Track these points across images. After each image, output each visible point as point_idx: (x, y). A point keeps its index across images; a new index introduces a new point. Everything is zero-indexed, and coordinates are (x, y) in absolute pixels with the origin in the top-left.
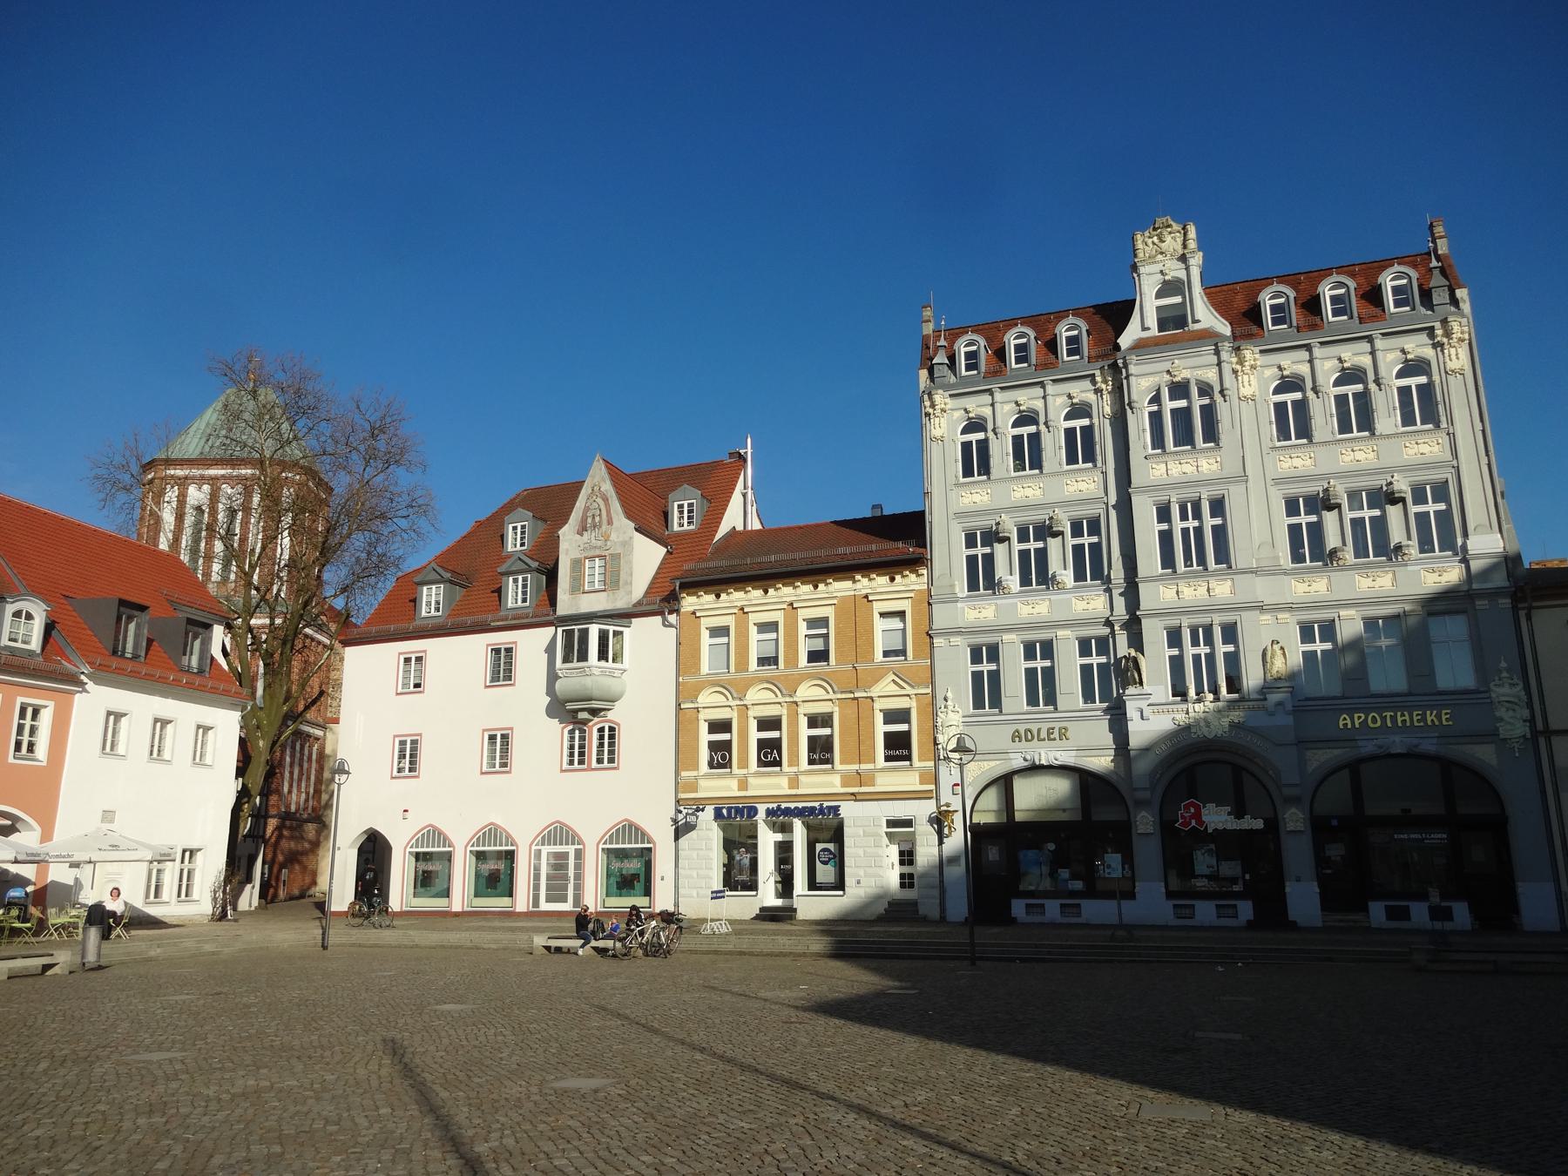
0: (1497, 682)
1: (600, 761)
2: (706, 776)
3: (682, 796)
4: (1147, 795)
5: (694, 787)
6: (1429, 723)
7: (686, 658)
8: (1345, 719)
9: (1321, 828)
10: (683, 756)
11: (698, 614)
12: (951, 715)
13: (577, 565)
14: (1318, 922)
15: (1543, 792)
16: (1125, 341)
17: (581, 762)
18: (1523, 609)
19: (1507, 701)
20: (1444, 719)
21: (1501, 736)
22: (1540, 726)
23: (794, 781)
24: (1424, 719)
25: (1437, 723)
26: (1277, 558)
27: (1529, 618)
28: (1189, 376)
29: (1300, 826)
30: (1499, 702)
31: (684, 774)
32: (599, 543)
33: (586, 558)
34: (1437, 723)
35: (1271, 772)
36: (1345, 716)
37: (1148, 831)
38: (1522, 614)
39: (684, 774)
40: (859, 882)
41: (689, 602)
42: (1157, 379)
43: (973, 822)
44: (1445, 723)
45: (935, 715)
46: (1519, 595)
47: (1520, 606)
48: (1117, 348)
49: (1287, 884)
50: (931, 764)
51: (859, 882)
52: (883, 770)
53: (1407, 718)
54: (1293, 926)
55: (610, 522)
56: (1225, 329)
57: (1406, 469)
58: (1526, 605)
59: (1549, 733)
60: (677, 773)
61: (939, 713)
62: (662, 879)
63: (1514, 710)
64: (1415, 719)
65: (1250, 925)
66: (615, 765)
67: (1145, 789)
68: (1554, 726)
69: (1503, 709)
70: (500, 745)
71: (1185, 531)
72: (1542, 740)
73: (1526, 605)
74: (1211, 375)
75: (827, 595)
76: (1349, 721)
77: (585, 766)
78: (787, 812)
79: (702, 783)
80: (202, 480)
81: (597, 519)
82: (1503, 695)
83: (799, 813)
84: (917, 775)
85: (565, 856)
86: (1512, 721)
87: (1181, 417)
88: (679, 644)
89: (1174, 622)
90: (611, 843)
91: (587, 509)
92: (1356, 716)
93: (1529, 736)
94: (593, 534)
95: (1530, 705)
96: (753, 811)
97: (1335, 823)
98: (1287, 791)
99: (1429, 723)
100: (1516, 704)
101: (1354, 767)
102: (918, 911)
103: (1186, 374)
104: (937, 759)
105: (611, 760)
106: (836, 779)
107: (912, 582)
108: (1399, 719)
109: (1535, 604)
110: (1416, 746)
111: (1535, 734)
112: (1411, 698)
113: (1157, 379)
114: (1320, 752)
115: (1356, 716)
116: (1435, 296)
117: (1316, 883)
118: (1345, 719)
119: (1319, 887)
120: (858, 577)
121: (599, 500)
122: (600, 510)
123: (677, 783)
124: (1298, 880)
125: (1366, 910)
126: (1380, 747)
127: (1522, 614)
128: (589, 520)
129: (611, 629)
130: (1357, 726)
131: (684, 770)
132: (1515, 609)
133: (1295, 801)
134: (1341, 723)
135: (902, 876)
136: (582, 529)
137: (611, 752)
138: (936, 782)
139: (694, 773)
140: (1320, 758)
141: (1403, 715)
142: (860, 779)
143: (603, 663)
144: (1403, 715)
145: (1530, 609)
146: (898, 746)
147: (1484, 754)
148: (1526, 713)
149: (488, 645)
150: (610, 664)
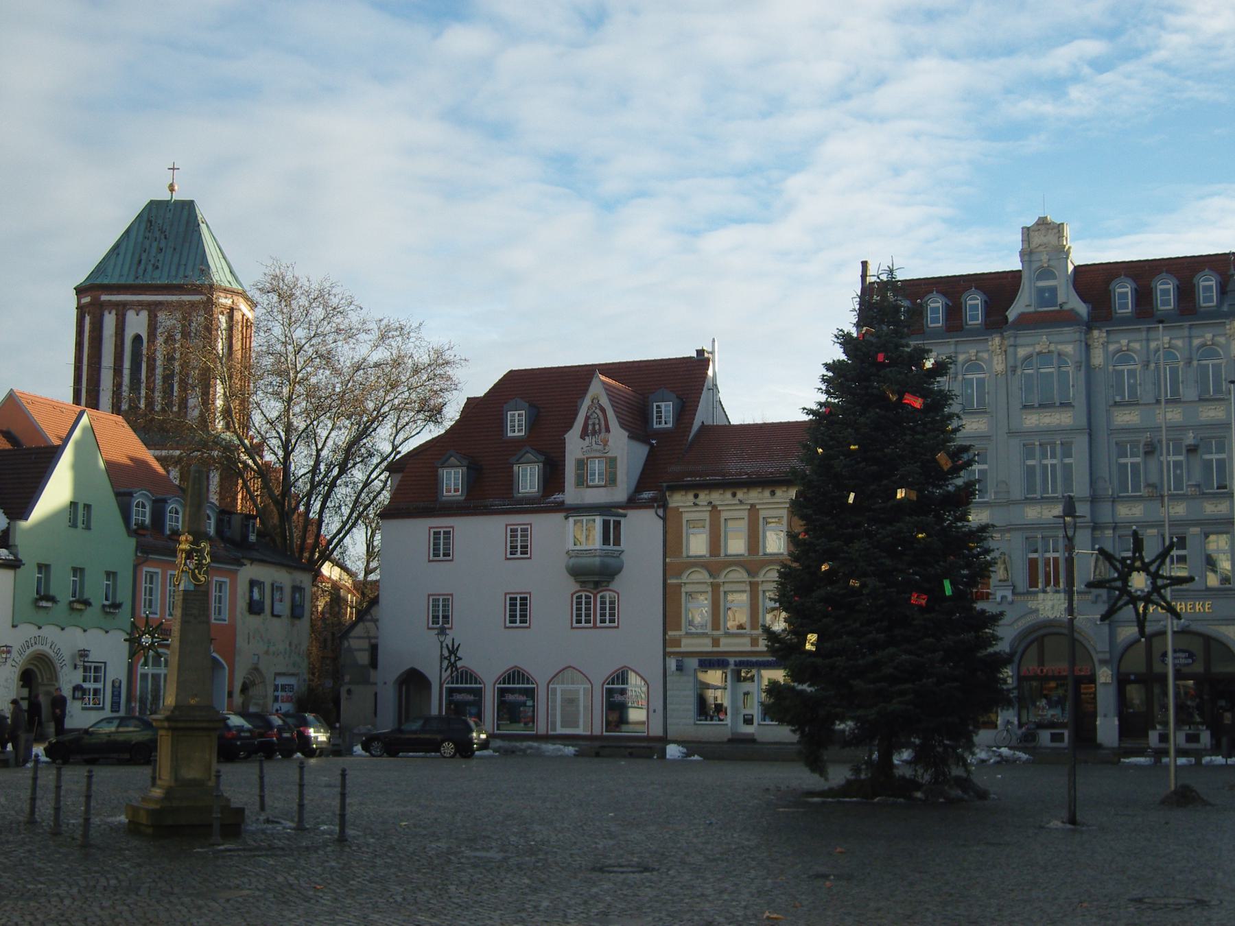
1: (603, 621)
3: (668, 650)
5: (677, 642)
6: (1197, 610)
7: (672, 543)
9: (1122, 682)
13: (581, 464)
16: (1012, 314)
17: (588, 621)
24: (1194, 607)
25: (1202, 610)
29: (1109, 680)
32: (599, 447)
33: (587, 459)
34: (1202, 610)
39: (670, 633)
44: (1207, 610)
53: (1183, 606)
54: (1100, 746)
55: (608, 430)
56: (1082, 309)
62: (654, 711)
64: (1189, 607)
70: (518, 609)
74: (1069, 349)
77: (591, 625)
79: (684, 641)
80: (140, 305)
81: (597, 427)
89: (1029, 534)
91: (587, 418)
94: (594, 440)
97: (1132, 677)
99: (1197, 610)
103: (1052, 347)
105: (612, 621)
110: (1188, 626)
114: (1127, 629)
121: (598, 411)
122: (599, 420)
123: (665, 640)
125: (1147, 736)
129: (612, 519)
136: (584, 434)
137: (612, 615)
143: (606, 547)
149: (507, 526)
150: (611, 547)
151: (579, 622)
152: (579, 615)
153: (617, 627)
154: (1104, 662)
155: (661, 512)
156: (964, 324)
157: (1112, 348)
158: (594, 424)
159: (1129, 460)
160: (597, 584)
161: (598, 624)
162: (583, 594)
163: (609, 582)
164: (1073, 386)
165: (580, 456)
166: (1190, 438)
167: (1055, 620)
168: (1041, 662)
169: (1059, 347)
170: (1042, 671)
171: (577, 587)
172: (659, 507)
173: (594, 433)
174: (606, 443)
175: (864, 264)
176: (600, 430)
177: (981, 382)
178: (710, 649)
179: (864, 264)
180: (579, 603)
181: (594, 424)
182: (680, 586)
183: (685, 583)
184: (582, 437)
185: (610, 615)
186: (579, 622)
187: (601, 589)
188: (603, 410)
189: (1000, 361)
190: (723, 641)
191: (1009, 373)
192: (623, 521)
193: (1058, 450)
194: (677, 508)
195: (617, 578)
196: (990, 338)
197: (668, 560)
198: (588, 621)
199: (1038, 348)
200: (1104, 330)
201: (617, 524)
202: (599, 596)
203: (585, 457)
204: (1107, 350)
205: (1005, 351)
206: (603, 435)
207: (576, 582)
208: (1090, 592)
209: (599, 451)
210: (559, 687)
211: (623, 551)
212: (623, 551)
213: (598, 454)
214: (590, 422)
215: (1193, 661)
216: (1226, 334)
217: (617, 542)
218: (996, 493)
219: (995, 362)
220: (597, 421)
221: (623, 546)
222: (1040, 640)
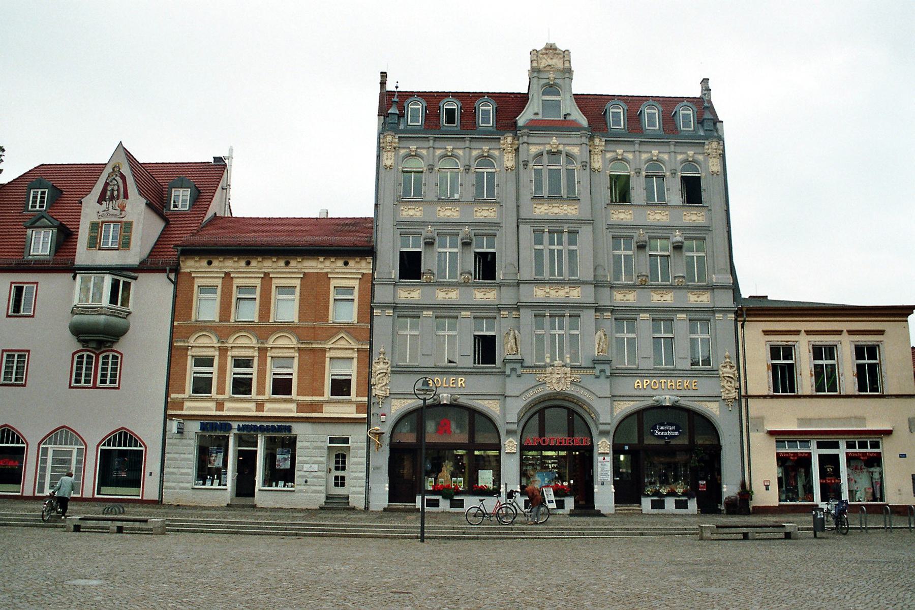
0: (724, 365)
2: (190, 399)
3: (170, 412)
4: (514, 427)
5: (180, 405)
8: (638, 382)
10: (172, 381)
11: (193, 275)
12: (381, 365)
13: (95, 227)
14: (613, 512)
15: (741, 432)
16: (522, 120)
17: (87, 381)
18: (740, 321)
19: (728, 377)
20: (693, 385)
21: (723, 398)
22: (743, 393)
23: (220, 405)
26: (606, 276)
27: (743, 327)
28: (562, 149)
30: (724, 377)
31: (173, 396)
33: (103, 222)
35: (593, 415)
36: (638, 380)
37: (513, 451)
38: (739, 324)
39: (173, 396)
40: (306, 482)
41: (189, 266)
42: (541, 148)
43: (394, 441)
45: (370, 365)
46: (739, 312)
47: (739, 319)
48: (516, 123)
49: (596, 486)
50: (366, 399)
51: (306, 482)
52: (327, 402)
54: (599, 514)
55: (126, 196)
56: (584, 121)
57: (682, 229)
58: (742, 319)
59: (747, 397)
60: (167, 395)
61: (373, 362)
62: (151, 474)
63: (731, 382)
65: (572, 514)
66: (117, 385)
67: (514, 423)
68: (749, 394)
69: (726, 381)
71: (552, 251)
72: (743, 400)
73: (742, 319)
74: (575, 150)
75: (296, 270)
76: (640, 384)
78: (255, 429)
79: (187, 404)
81: (116, 193)
82: (727, 373)
83: (262, 429)
84: (354, 406)
85: (70, 453)
86: (729, 388)
87: (554, 176)
88: (175, 296)
90: (109, 445)
91: (107, 184)
92: (645, 381)
93: (737, 398)
95: (739, 379)
96: (228, 428)
97: (627, 448)
98: (602, 428)
100: (732, 378)
101: (639, 414)
102: (348, 503)
103: (561, 148)
104: (369, 396)
106: (293, 406)
107: (364, 266)
108: (669, 384)
109: (747, 319)
111: (740, 396)
112: (675, 372)
113: (541, 148)
114: (622, 403)
115: (645, 381)
116: (705, 124)
117: (613, 486)
118: (638, 382)
119: (614, 489)
120: (321, 259)
121: (118, 178)
122: (118, 186)
123: (166, 402)
124: (603, 484)
126: (657, 401)
127: (739, 324)
128: (109, 193)
129: (122, 280)
130: (645, 387)
131: (172, 393)
132: (736, 320)
133: (604, 433)
134: (636, 385)
135: (336, 478)
137: (114, 376)
138: (369, 413)
139: (181, 396)
140: (625, 407)
141: (671, 382)
142: (316, 406)
143: (113, 306)
144: (671, 382)
145: (744, 321)
146: (341, 387)
147: (712, 409)
148: (737, 385)
149: (12, 283)
151: (78, 381)
152: (79, 375)
153: (118, 388)
154: (510, 433)
155: (172, 276)
156: (477, 126)
157: (609, 155)
158: (113, 190)
159: (622, 252)
160: (101, 344)
161: (98, 384)
162: (85, 354)
163: (113, 343)
164: (579, 182)
165: (96, 220)
166: (678, 237)
167: (558, 393)
168: (542, 432)
169: (567, 148)
170: (544, 441)
171: (79, 347)
172: (171, 271)
173: (112, 198)
174: (123, 209)
175: (384, 75)
176: (118, 196)
177: (491, 175)
178: (214, 413)
179: (384, 75)
180: (80, 363)
181: (113, 190)
182: (187, 348)
183: (192, 347)
184: (100, 202)
185: (110, 379)
186: (78, 381)
187: (103, 349)
188: (123, 177)
189: (510, 159)
190: (227, 405)
191: (521, 167)
192: (133, 283)
193: (565, 237)
194: (190, 273)
195: (123, 340)
196: (502, 138)
197: (176, 323)
198: (87, 381)
199: (548, 148)
200: (604, 139)
201: (127, 286)
202: (101, 357)
203: (100, 220)
204: (605, 158)
205: (517, 150)
206: (121, 200)
207: (78, 341)
208: (595, 368)
209: (116, 215)
210: (51, 448)
211: (130, 313)
212: (130, 313)
213: (114, 219)
214: (109, 188)
215: (679, 433)
216: (704, 153)
217: (125, 302)
218: (504, 274)
219: (506, 159)
220: (116, 188)
221: (131, 306)
222: (541, 412)
